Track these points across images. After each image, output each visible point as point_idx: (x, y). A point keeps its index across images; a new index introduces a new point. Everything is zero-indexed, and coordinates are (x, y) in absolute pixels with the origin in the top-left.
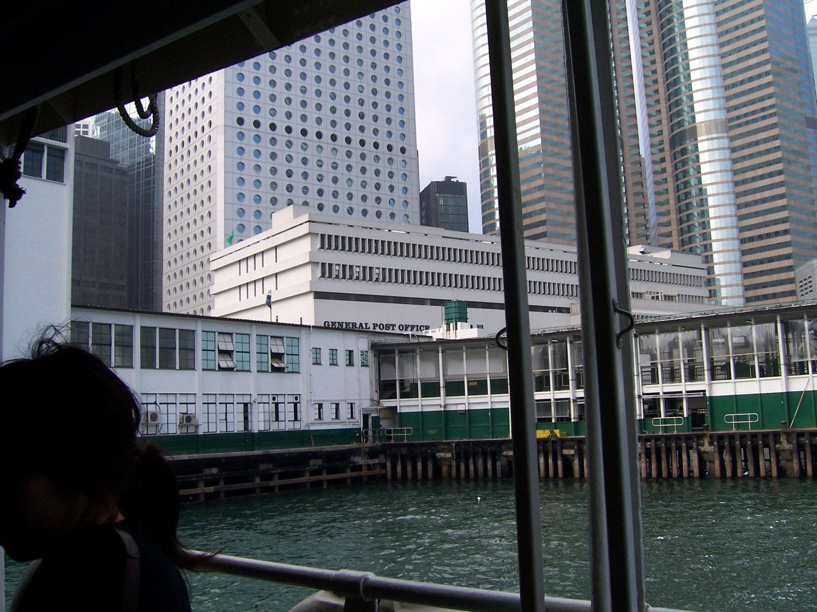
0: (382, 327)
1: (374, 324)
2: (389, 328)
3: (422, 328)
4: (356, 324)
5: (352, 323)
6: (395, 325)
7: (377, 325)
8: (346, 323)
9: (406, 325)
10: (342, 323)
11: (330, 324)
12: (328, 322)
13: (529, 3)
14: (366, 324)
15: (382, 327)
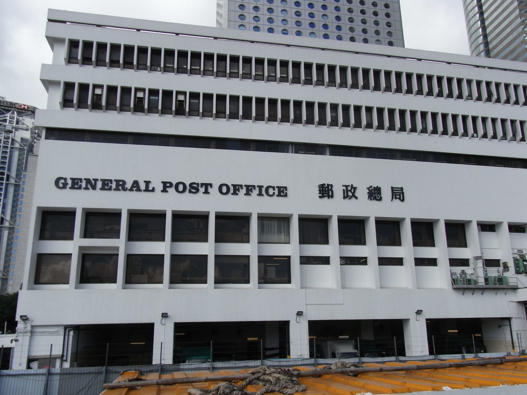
0: (181, 188)
1: (164, 183)
2: (197, 191)
3: (271, 191)
4: (124, 182)
5: (117, 181)
6: (211, 185)
7: (171, 185)
8: (103, 181)
9: (234, 186)
10: (96, 180)
11: (70, 182)
12: (65, 179)
13: (516, 4)
14: (147, 183)
15: (181, 188)
